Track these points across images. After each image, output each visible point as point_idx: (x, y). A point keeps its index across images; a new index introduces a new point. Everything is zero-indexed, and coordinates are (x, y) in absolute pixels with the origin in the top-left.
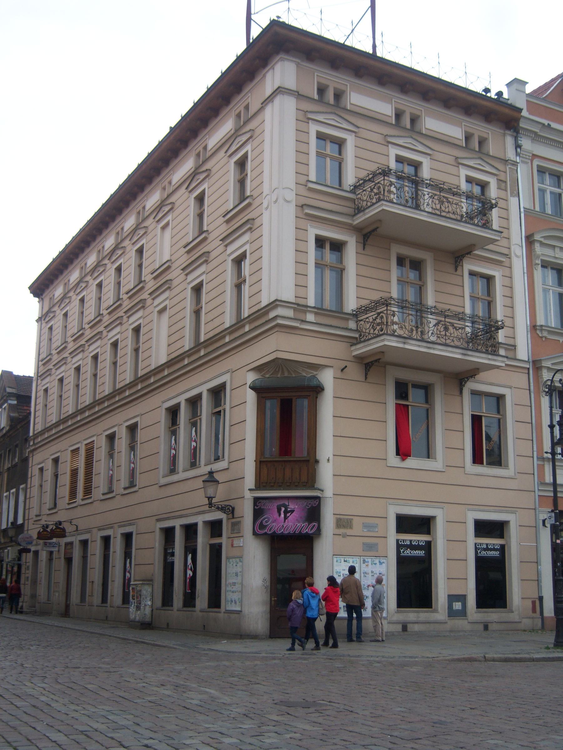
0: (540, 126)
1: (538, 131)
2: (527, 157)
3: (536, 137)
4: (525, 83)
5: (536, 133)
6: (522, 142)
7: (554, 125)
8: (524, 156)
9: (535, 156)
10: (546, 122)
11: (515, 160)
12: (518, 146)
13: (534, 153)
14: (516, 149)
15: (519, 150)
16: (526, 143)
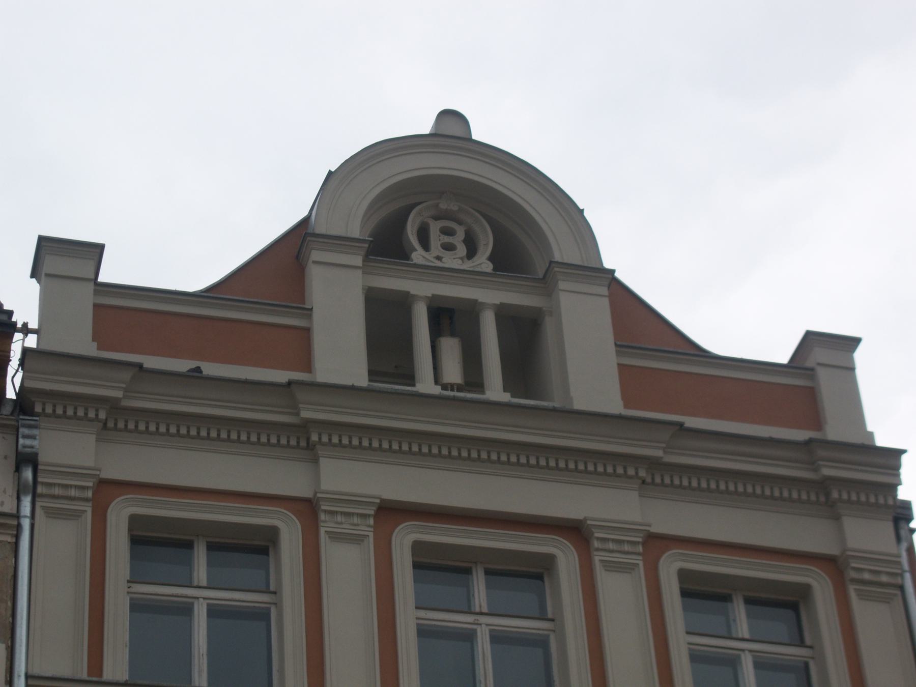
0: (127, 375)
1: (119, 394)
2: (73, 493)
3: (113, 421)
4: (95, 251)
5: (113, 406)
6: (35, 443)
7: (210, 369)
8: (57, 491)
9: (107, 489)
10: (182, 365)
11: (9, 507)
12: (26, 459)
13: (106, 474)
14: (18, 469)
15: (28, 474)
16: (66, 448)
